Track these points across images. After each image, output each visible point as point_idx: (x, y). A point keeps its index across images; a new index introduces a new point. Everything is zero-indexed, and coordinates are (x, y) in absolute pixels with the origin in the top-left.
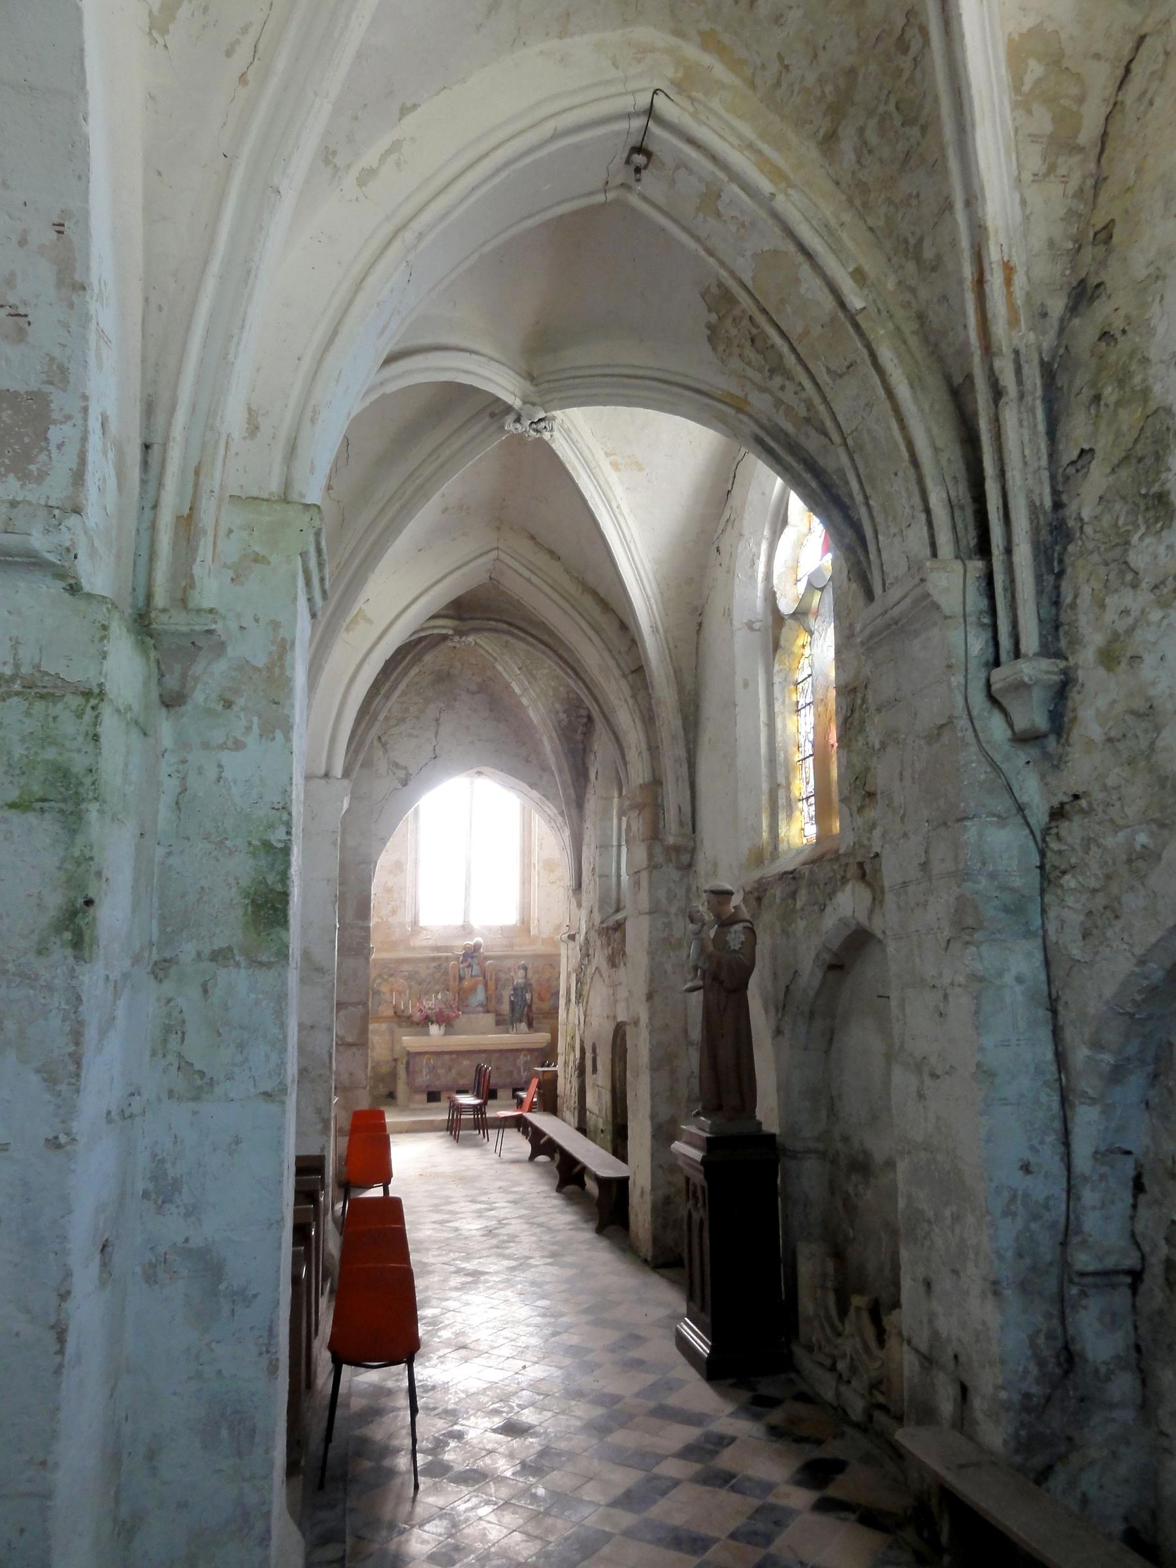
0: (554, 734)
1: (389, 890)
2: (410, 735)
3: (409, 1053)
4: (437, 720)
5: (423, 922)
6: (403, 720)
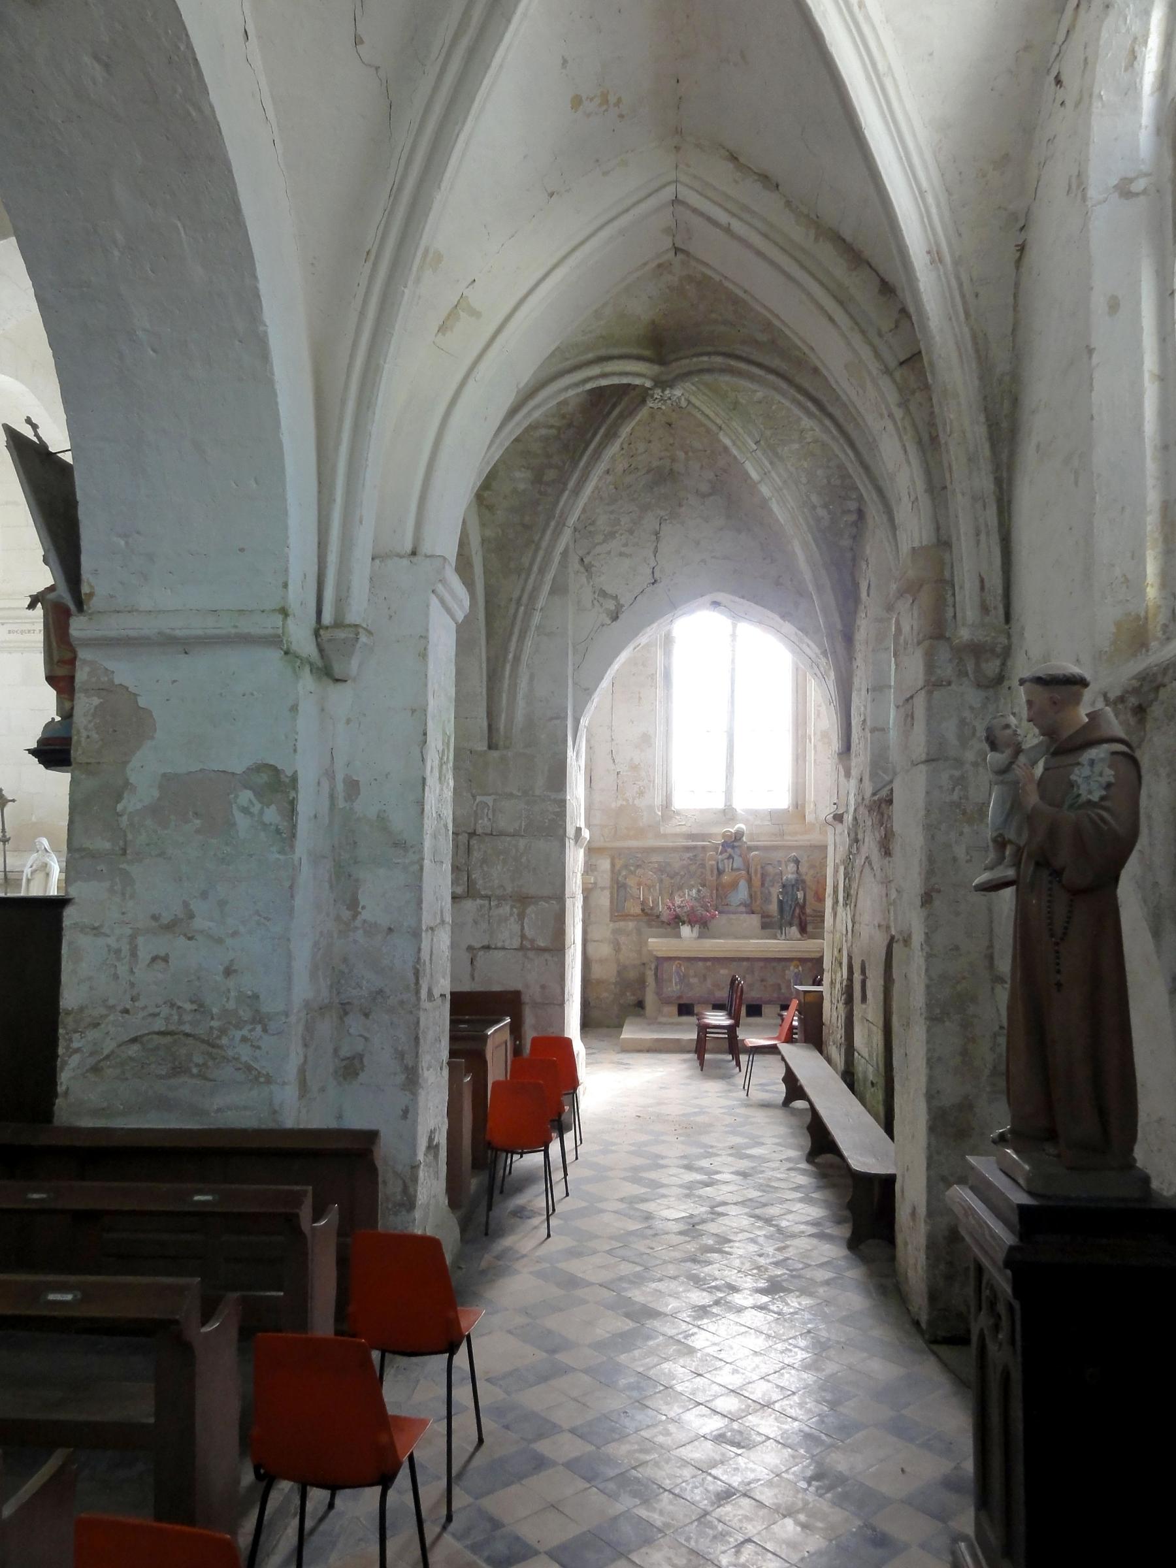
0: (809, 537)
1: (635, 768)
2: (621, 554)
3: (658, 958)
4: (657, 534)
5: (678, 803)
6: (612, 535)
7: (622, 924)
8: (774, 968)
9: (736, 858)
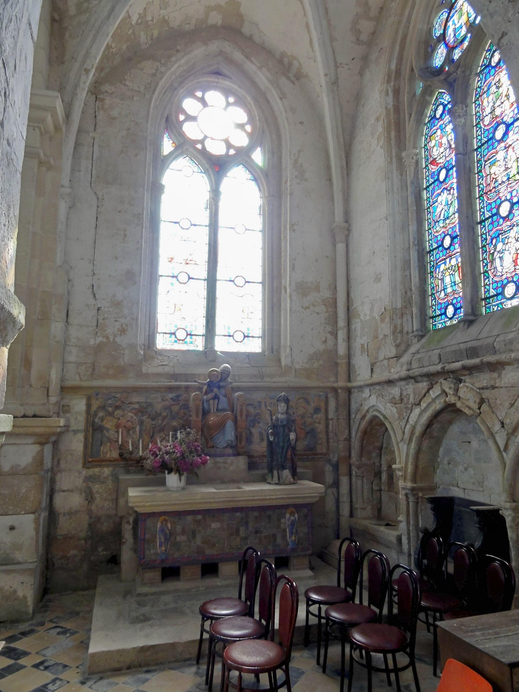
1: (117, 304)
7: (97, 470)
8: (269, 517)
9: (222, 398)
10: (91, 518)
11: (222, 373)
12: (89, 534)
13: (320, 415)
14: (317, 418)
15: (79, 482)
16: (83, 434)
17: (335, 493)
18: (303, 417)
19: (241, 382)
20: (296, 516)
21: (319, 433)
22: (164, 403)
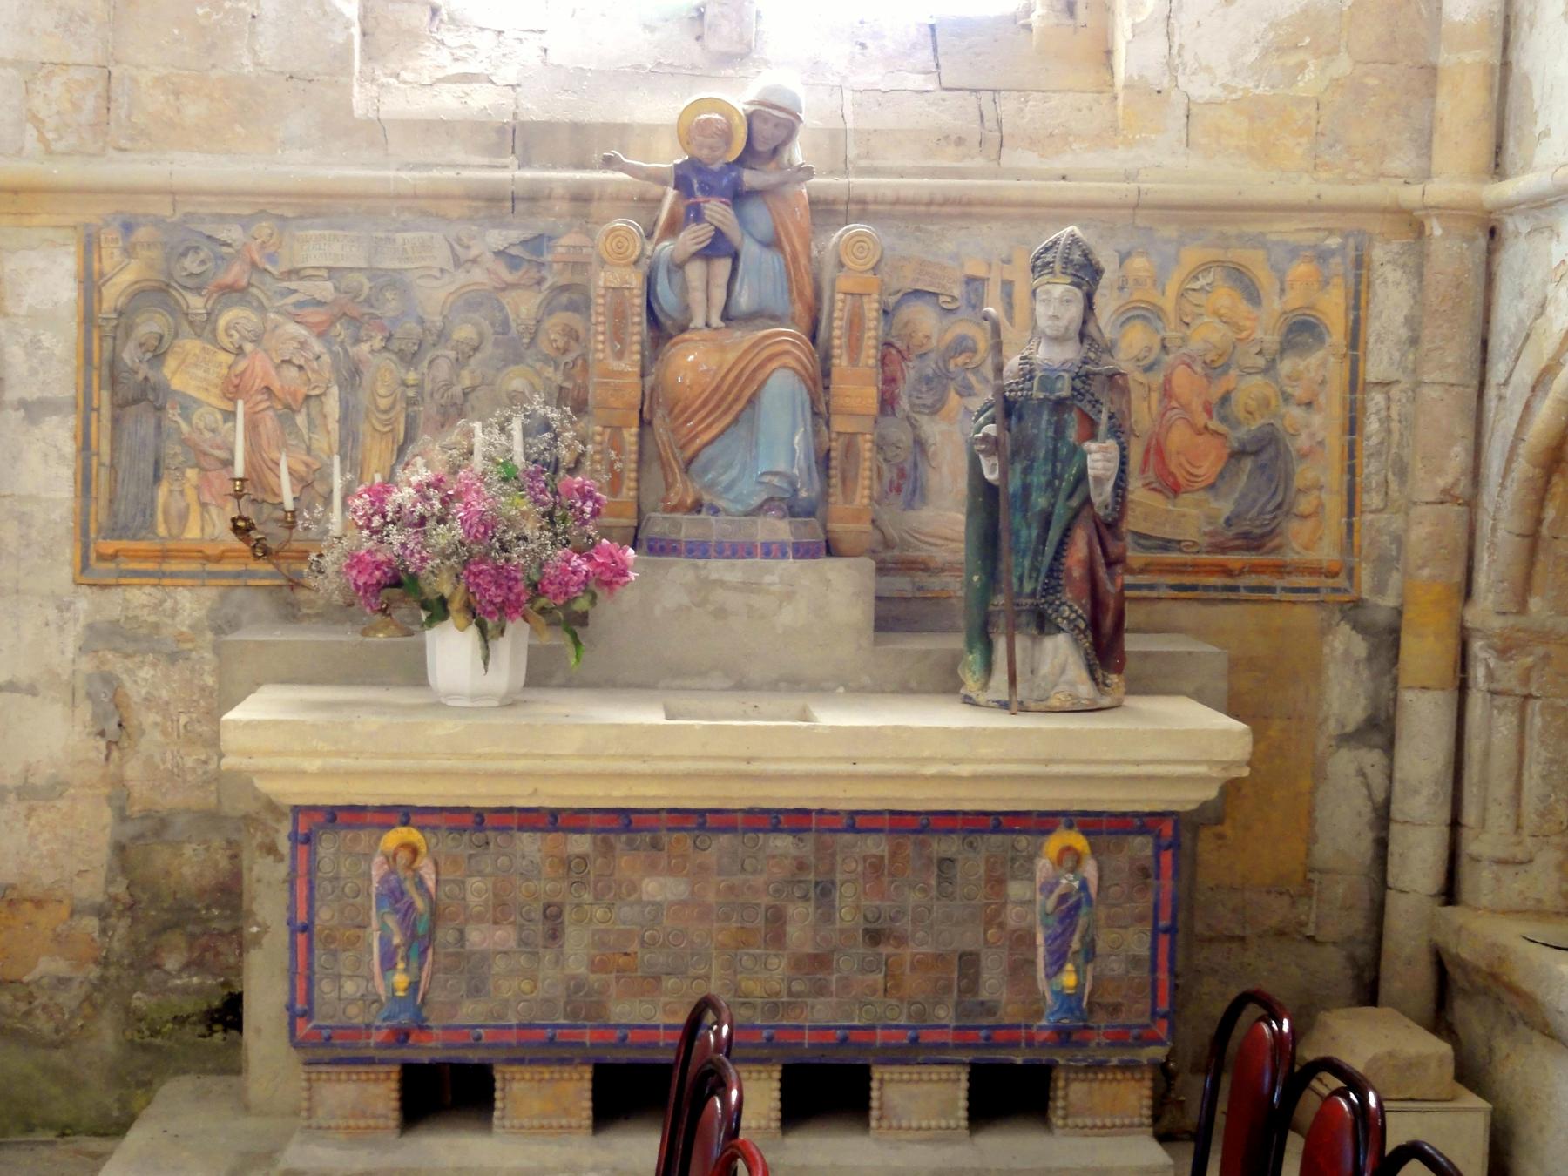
7: (140, 597)
9: (750, 250)
10: (122, 817)
11: (750, 118)
12: (120, 889)
13: (1314, 359)
14: (1294, 378)
15: (63, 651)
16: (72, 421)
17: (1378, 781)
18: (1215, 367)
19: (873, 172)
20: (1090, 870)
21: (1304, 456)
22: (461, 277)
